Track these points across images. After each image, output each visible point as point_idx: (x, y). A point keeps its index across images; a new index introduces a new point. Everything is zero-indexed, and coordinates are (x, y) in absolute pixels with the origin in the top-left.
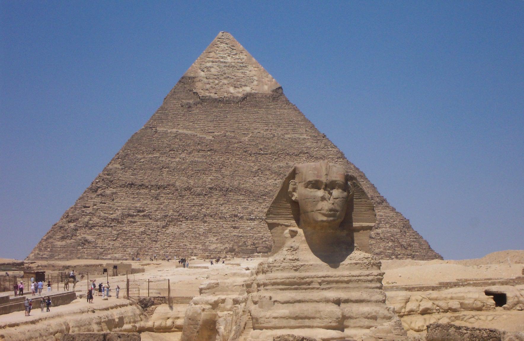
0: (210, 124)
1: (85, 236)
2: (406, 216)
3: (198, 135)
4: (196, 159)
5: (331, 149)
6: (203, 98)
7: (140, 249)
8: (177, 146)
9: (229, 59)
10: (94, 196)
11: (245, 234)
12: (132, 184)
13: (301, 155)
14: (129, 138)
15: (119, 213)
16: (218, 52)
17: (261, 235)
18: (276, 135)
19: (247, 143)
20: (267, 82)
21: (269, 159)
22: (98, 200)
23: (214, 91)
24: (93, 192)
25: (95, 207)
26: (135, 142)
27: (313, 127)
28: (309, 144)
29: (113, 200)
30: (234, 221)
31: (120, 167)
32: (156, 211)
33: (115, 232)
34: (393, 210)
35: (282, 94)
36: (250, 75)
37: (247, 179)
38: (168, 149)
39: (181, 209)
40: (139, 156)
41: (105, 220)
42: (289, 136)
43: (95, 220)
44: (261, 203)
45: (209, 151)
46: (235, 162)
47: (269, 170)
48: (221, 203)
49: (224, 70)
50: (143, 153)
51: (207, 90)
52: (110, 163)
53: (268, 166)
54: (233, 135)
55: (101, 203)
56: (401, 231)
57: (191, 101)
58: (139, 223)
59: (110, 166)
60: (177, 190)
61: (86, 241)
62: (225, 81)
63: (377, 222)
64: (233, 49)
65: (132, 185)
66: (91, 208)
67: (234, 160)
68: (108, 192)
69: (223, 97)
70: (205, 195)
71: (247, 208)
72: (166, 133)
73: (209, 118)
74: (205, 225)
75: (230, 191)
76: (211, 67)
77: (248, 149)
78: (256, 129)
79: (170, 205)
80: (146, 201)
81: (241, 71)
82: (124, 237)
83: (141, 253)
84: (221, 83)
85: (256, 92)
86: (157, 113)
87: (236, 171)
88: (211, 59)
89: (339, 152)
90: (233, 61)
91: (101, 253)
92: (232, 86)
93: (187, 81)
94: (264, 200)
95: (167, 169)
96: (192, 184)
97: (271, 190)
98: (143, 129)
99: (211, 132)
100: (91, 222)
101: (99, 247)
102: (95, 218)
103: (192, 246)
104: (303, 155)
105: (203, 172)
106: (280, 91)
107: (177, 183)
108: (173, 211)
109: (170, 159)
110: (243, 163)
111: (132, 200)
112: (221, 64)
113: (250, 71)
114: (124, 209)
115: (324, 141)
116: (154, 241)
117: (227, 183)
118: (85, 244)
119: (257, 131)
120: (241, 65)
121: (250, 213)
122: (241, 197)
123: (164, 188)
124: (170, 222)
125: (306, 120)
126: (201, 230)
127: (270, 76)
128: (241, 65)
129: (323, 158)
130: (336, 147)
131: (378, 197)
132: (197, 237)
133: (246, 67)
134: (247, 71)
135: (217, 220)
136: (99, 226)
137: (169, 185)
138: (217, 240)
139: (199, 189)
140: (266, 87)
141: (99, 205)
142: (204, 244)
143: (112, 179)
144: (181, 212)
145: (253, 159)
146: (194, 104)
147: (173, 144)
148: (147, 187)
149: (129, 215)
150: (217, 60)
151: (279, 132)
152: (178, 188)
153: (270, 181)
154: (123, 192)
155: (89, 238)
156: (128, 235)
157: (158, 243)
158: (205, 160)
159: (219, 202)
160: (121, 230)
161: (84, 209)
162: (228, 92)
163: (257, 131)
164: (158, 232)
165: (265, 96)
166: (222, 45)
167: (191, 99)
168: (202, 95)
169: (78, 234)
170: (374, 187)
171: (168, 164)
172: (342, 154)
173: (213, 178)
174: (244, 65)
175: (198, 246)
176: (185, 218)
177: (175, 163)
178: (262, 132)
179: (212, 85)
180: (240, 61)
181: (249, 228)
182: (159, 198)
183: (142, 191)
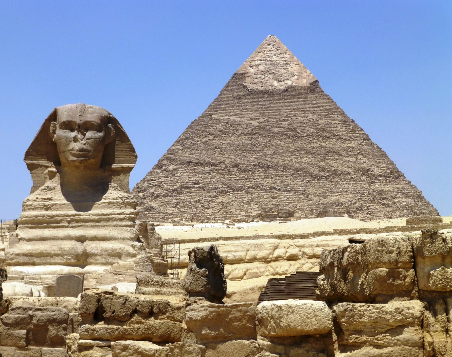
0: (257, 113)
1: (151, 203)
2: (419, 188)
3: (246, 121)
4: (243, 141)
5: (358, 132)
6: (251, 90)
7: (195, 214)
8: (227, 131)
9: (275, 58)
10: (159, 171)
11: (282, 203)
12: (190, 162)
13: (332, 137)
14: (189, 124)
15: (178, 185)
16: (265, 52)
17: (295, 204)
18: (311, 120)
19: (286, 127)
20: (306, 76)
21: (304, 141)
22: (162, 175)
23: (261, 84)
24: (158, 168)
25: (160, 180)
26: (195, 127)
27: (343, 114)
28: (339, 128)
29: (174, 175)
30: (272, 192)
31: (181, 148)
32: (209, 183)
33: (175, 201)
34: (409, 183)
35: (318, 86)
36: (292, 71)
37: (285, 158)
38: (220, 133)
39: (229, 183)
40: (197, 139)
41: (167, 191)
42: (323, 121)
43: (160, 191)
44: (295, 177)
45: (254, 134)
46: (276, 143)
47: (305, 149)
48: (263, 177)
49: (270, 67)
50: (200, 137)
51: (255, 83)
52: (174, 144)
53: (304, 147)
54: (275, 121)
55: (165, 177)
56: (415, 201)
57: (241, 94)
58: (194, 194)
59: (173, 147)
60: (226, 167)
61: (152, 207)
62: (271, 76)
63: (394, 193)
64: (278, 50)
65: (190, 162)
66: (157, 181)
67: (275, 141)
68: (171, 168)
69: (268, 89)
70: (250, 171)
71: (284, 182)
72: (219, 120)
73: (256, 107)
74: (249, 195)
75: (271, 167)
76: (259, 65)
77: (287, 133)
78: (295, 116)
79: (220, 179)
80: (201, 176)
81: (284, 67)
82: (182, 205)
83: (195, 218)
84: (267, 78)
85: (296, 84)
86: (213, 103)
87: (276, 151)
88: (260, 58)
89: (365, 134)
90: (278, 59)
91: (163, 218)
92: (276, 80)
93: (238, 77)
94: (299, 175)
95: (219, 150)
96: (239, 161)
97: (305, 166)
98: (200, 117)
99: (257, 119)
100: (156, 192)
101: (162, 212)
102: (160, 189)
103: (237, 213)
104: (334, 137)
105: (248, 152)
106: (317, 84)
107: (227, 161)
108: (223, 184)
109: (221, 141)
110: (282, 144)
111: (190, 174)
112: (268, 62)
113: (292, 67)
114: (183, 182)
115: (353, 125)
116: (207, 208)
117: (268, 161)
118: (151, 210)
119: (295, 117)
120: (285, 62)
121: (287, 186)
122: (280, 173)
123: (216, 166)
124: (220, 192)
125: (338, 108)
126: (245, 199)
127: (309, 71)
128: (285, 62)
129: (351, 139)
130: (362, 130)
131: (396, 172)
132: (241, 206)
133: (288, 64)
134: (290, 68)
135: (259, 192)
136: (163, 196)
137: (219, 163)
138: (258, 208)
139: (245, 166)
140: (305, 81)
141: (163, 179)
142: (247, 211)
143: (174, 158)
144: (229, 185)
145: (291, 140)
146: (244, 95)
147: (226, 129)
148: (202, 164)
149: (187, 187)
150: (265, 58)
151: (315, 118)
152: (227, 164)
153: (305, 159)
154: (183, 168)
155: (155, 205)
156: (185, 203)
157: (210, 210)
158: (250, 142)
159: (260, 176)
160: (180, 199)
161: (150, 182)
162: (272, 85)
163: (295, 117)
164: (210, 201)
165: (303, 88)
166: (269, 47)
167: (242, 91)
168: (251, 87)
169: (145, 202)
170: (393, 164)
171: (220, 145)
172: (367, 136)
173: (256, 156)
174: (287, 62)
175: (242, 213)
176: (232, 189)
177: (225, 145)
178: (300, 118)
179: (259, 79)
180: (283, 59)
181: (285, 198)
182: (212, 173)
183: (198, 168)
